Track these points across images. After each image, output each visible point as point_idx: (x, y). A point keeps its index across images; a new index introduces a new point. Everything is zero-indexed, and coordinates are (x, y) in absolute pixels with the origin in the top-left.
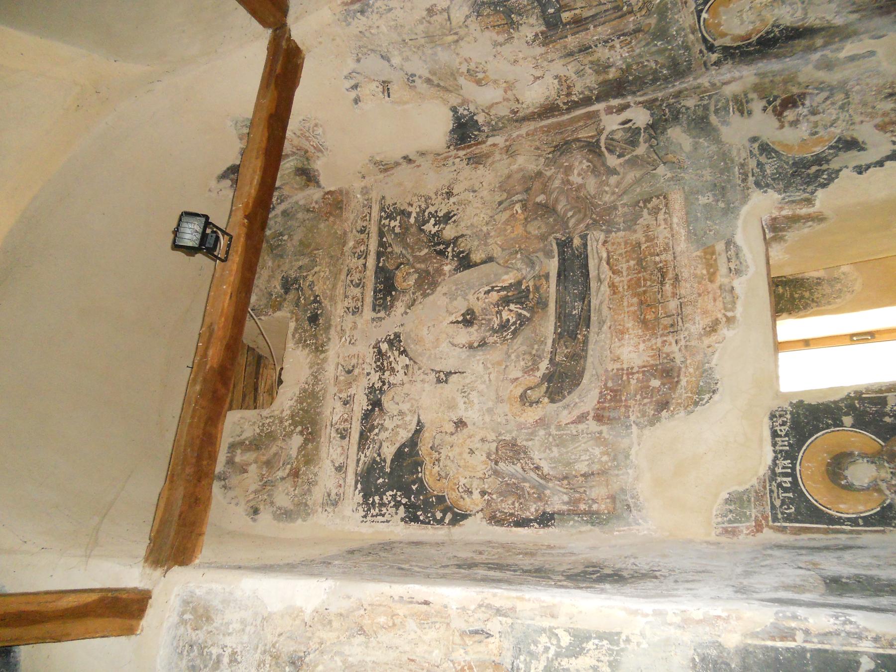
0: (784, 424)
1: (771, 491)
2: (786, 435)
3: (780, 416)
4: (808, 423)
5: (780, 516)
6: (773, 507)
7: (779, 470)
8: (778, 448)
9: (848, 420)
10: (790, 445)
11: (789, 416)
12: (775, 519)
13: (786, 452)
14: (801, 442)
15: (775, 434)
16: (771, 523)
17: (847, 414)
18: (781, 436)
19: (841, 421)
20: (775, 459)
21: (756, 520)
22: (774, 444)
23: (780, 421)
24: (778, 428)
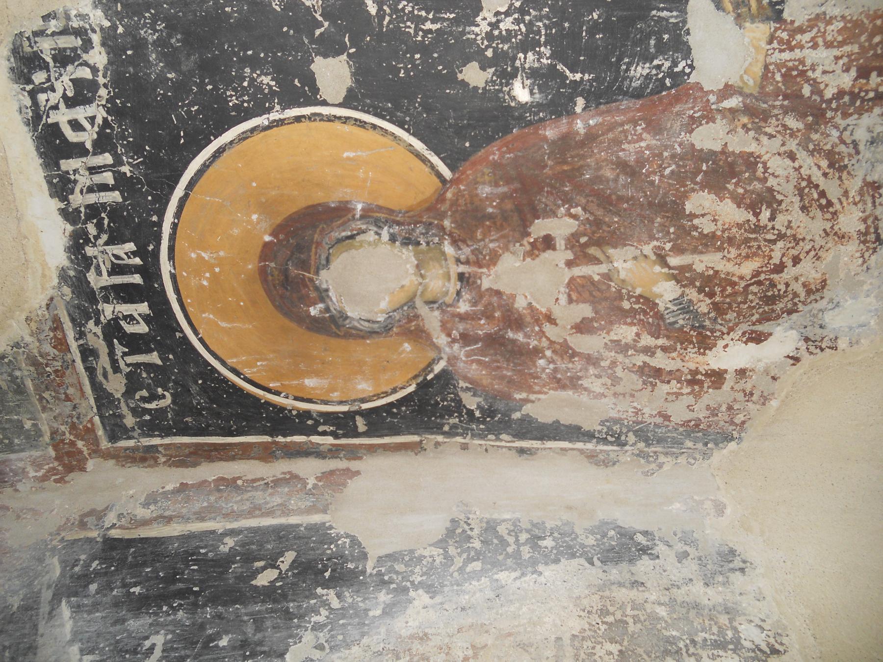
0: (82, 93)
1: (87, 353)
2: (102, 144)
3: (63, 59)
4: (181, 87)
5: (130, 421)
6: (103, 398)
7: (98, 280)
8: (78, 200)
9: (333, 74)
10: (122, 183)
11: (98, 57)
12: (116, 431)
13: (115, 211)
14: (161, 174)
15: (53, 146)
16: (105, 444)
17: (330, 47)
18: (79, 150)
19: (310, 80)
20: (78, 245)
21: (57, 442)
22: (61, 187)
23: (64, 84)
24: (62, 117)
